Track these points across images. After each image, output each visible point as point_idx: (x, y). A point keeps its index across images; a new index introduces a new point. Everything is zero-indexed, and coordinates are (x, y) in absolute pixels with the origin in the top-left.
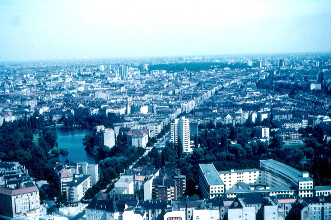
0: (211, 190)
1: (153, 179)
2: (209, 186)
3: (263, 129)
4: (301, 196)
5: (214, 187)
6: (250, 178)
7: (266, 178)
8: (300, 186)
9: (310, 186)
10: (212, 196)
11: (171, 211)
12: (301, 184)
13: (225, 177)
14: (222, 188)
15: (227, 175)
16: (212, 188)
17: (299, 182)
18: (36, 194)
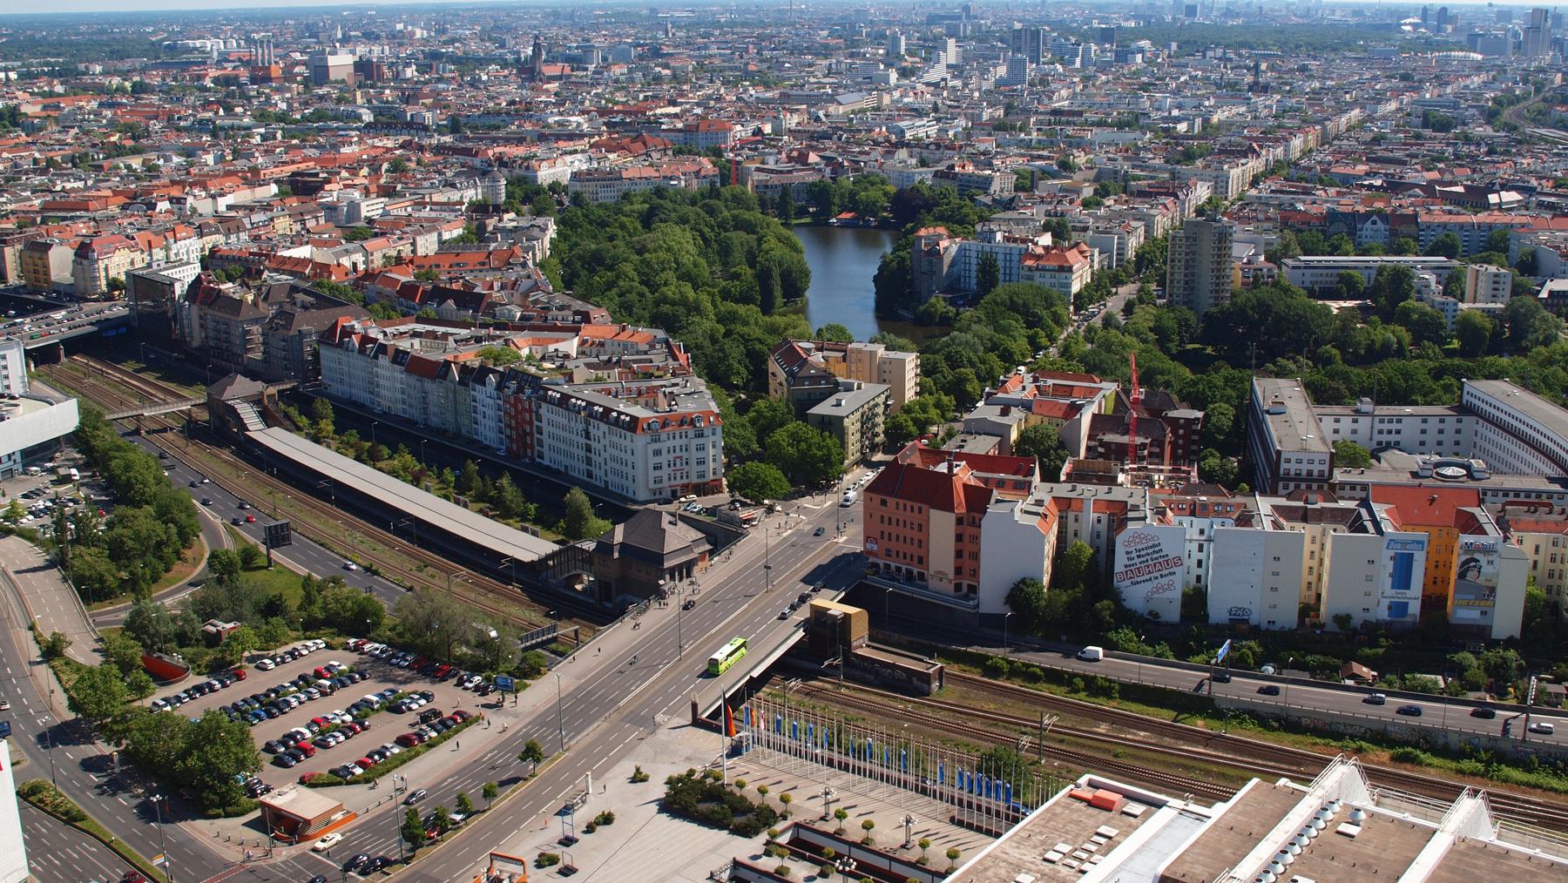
1: (1094, 415)
6: (1423, 438)
18: (714, 434)
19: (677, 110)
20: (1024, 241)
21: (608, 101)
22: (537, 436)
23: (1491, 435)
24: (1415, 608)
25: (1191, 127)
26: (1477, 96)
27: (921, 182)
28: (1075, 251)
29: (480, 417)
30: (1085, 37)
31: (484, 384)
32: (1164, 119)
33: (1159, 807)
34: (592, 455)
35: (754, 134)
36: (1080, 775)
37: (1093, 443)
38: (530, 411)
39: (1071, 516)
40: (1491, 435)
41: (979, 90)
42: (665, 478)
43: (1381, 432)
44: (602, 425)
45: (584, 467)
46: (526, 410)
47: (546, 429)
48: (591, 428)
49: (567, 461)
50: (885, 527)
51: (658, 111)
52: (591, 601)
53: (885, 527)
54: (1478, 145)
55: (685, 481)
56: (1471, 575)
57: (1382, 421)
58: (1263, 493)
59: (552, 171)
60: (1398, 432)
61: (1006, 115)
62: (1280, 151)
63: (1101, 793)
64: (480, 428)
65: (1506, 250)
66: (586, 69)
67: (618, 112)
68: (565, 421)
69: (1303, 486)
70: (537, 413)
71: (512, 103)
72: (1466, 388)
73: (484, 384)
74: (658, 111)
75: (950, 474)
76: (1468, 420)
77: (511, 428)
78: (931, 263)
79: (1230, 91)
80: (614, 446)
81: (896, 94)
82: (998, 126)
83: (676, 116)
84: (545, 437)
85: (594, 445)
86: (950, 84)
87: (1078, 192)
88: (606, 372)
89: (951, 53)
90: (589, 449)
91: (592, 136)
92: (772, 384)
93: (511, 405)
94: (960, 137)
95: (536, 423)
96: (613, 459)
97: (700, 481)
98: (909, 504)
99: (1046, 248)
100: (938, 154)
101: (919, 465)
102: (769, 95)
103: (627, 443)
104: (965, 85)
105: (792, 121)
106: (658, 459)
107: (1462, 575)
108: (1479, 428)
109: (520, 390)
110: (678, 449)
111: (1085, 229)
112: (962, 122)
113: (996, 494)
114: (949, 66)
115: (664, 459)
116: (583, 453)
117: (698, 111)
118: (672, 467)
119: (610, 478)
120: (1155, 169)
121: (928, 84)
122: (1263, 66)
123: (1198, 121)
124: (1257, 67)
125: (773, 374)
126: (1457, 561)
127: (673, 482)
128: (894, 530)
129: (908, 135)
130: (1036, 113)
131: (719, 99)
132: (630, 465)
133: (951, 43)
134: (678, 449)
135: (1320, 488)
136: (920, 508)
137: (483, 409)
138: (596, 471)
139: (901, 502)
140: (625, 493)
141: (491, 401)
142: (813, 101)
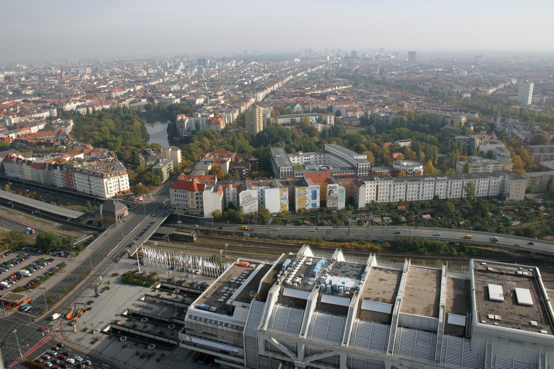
0: (281, 171)
1: (230, 162)
2: (279, 168)
3: (328, 117)
4: (360, 175)
5: (283, 168)
6: (316, 160)
7: (330, 160)
8: (359, 167)
9: (367, 167)
10: (282, 176)
11: (245, 189)
12: (360, 165)
13: (294, 159)
14: (291, 169)
15: (296, 158)
16: (282, 169)
17: (358, 164)
19: (106, 86)
20: (207, 116)
21: (85, 85)
23: (333, 158)
24: (318, 205)
25: (248, 83)
26: (321, 70)
27: (177, 102)
28: (220, 118)
29: (56, 179)
30: (218, 60)
31: (56, 169)
32: (241, 81)
33: (259, 264)
35: (128, 92)
36: (238, 258)
37: (231, 169)
38: (71, 175)
39: (227, 189)
40: (333, 158)
41: (190, 76)
43: (305, 159)
44: (93, 177)
47: (77, 180)
48: (90, 179)
49: (83, 189)
50: (177, 198)
51: (100, 87)
53: (177, 198)
54: (322, 83)
56: (331, 194)
57: (305, 157)
58: (276, 178)
59: (70, 106)
60: (309, 159)
61: (198, 82)
62: (272, 88)
63: (243, 262)
64: (57, 182)
65: (331, 111)
66: (77, 76)
67: (88, 88)
68: (82, 177)
69: (287, 176)
71: (56, 87)
72: (326, 146)
73: (56, 169)
74: (100, 87)
75: (193, 181)
76: (326, 155)
78: (182, 125)
79: (259, 73)
81: (168, 79)
82: (197, 86)
83: (105, 88)
84: (76, 182)
85: (91, 183)
86: (182, 75)
87: (220, 102)
88: (93, 163)
89: (182, 66)
90: (90, 185)
91: (81, 95)
92: (141, 161)
94: (186, 89)
95: (73, 179)
96: (97, 186)
98: (182, 191)
99: (213, 118)
100: (181, 94)
101: (184, 180)
102: (132, 81)
104: (187, 75)
105: (139, 88)
106: (110, 185)
107: (329, 195)
108: (329, 156)
109: (68, 170)
111: (223, 112)
112: (186, 85)
113: (206, 186)
114: (182, 70)
115: (112, 185)
116: (89, 186)
117: (112, 86)
119: (97, 192)
120: (239, 94)
121: (176, 75)
122: (266, 66)
123: (250, 82)
124: (264, 66)
125: (141, 159)
126: (328, 190)
127: (115, 191)
128: (179, 198)
129: (172, 89)
130: (206, 81)
131: (117, 82)
133: (182, 63)
135: (291, 175)
136: (186, 192)
138: (92, 191)
139: (180, 190)
141: (59, 174)
142: (145, 81)
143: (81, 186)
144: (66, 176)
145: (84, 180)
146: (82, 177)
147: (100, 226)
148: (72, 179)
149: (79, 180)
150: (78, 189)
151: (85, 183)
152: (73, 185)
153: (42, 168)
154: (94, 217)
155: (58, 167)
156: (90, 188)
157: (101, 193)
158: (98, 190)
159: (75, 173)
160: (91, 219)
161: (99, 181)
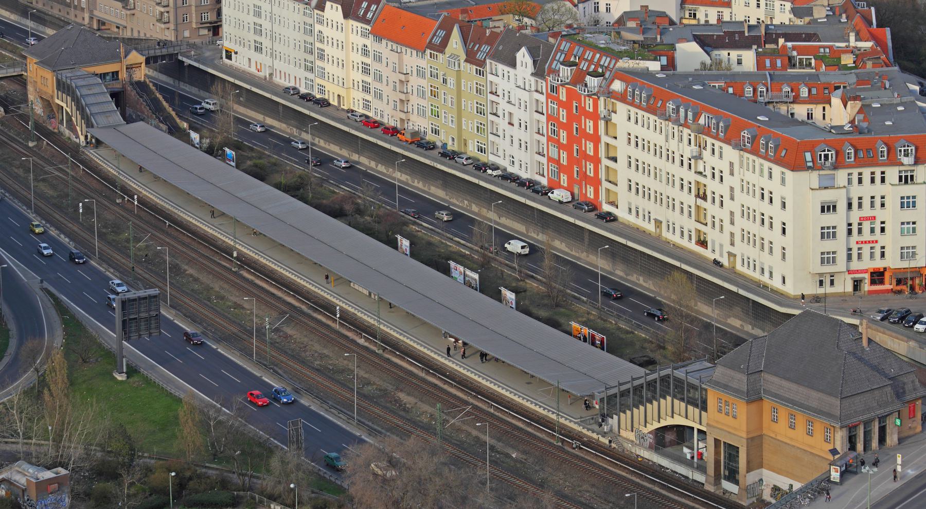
22: (605, 162)
29: (502, 123)
31: (513, 64)
34: (707, 205)
38: (595, 116)
42: (842, 257)
44: (728, 150)
45: (691, 225)
46: (589, 115)
47: (623, 150)
49: (659, 212)
52: (699, 477)
55: (879, 264)
68: (657, 139)
70: (607, 121)
73: (513, 64)
77: (560, 146)
80: (746, 188)
85: (712, 186)
88: (734, 54)
93: (561, 104)
95: (605, 139)
96: (746, 212)
97: (905, 264)
103: (773, 185)
109: (578, 79)
110: (866, 202)
116: (690, 200)
118: (855, 236)
119: (740, 249)
127: (855, 265)
132: (778, 227)
134: (866, 202)
137: (509, 108)
138: (712, 235)
140: (765, 279)
141: (525, 96)
143: (646, 194)
144: (563, 115)
145: (670, 158)
146: (657, 139)
147: (733, 476)
148: (596, 139)
149: (637, 154)
150: (621, 213)
151: (670, 180)
152: (596, 183)
153: (431, 46)
154: (704, 408)
155: (523, 56)
156: (700, 216)
157: (766, 259)
158: (748, 238)
159: (621, 107)
160: (679, 421)
161: (764, 182)
